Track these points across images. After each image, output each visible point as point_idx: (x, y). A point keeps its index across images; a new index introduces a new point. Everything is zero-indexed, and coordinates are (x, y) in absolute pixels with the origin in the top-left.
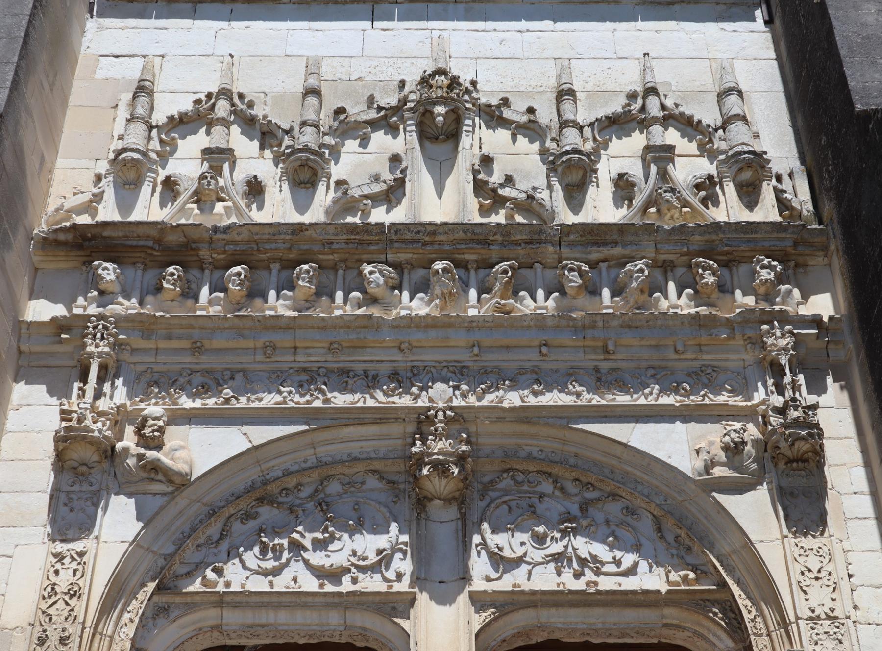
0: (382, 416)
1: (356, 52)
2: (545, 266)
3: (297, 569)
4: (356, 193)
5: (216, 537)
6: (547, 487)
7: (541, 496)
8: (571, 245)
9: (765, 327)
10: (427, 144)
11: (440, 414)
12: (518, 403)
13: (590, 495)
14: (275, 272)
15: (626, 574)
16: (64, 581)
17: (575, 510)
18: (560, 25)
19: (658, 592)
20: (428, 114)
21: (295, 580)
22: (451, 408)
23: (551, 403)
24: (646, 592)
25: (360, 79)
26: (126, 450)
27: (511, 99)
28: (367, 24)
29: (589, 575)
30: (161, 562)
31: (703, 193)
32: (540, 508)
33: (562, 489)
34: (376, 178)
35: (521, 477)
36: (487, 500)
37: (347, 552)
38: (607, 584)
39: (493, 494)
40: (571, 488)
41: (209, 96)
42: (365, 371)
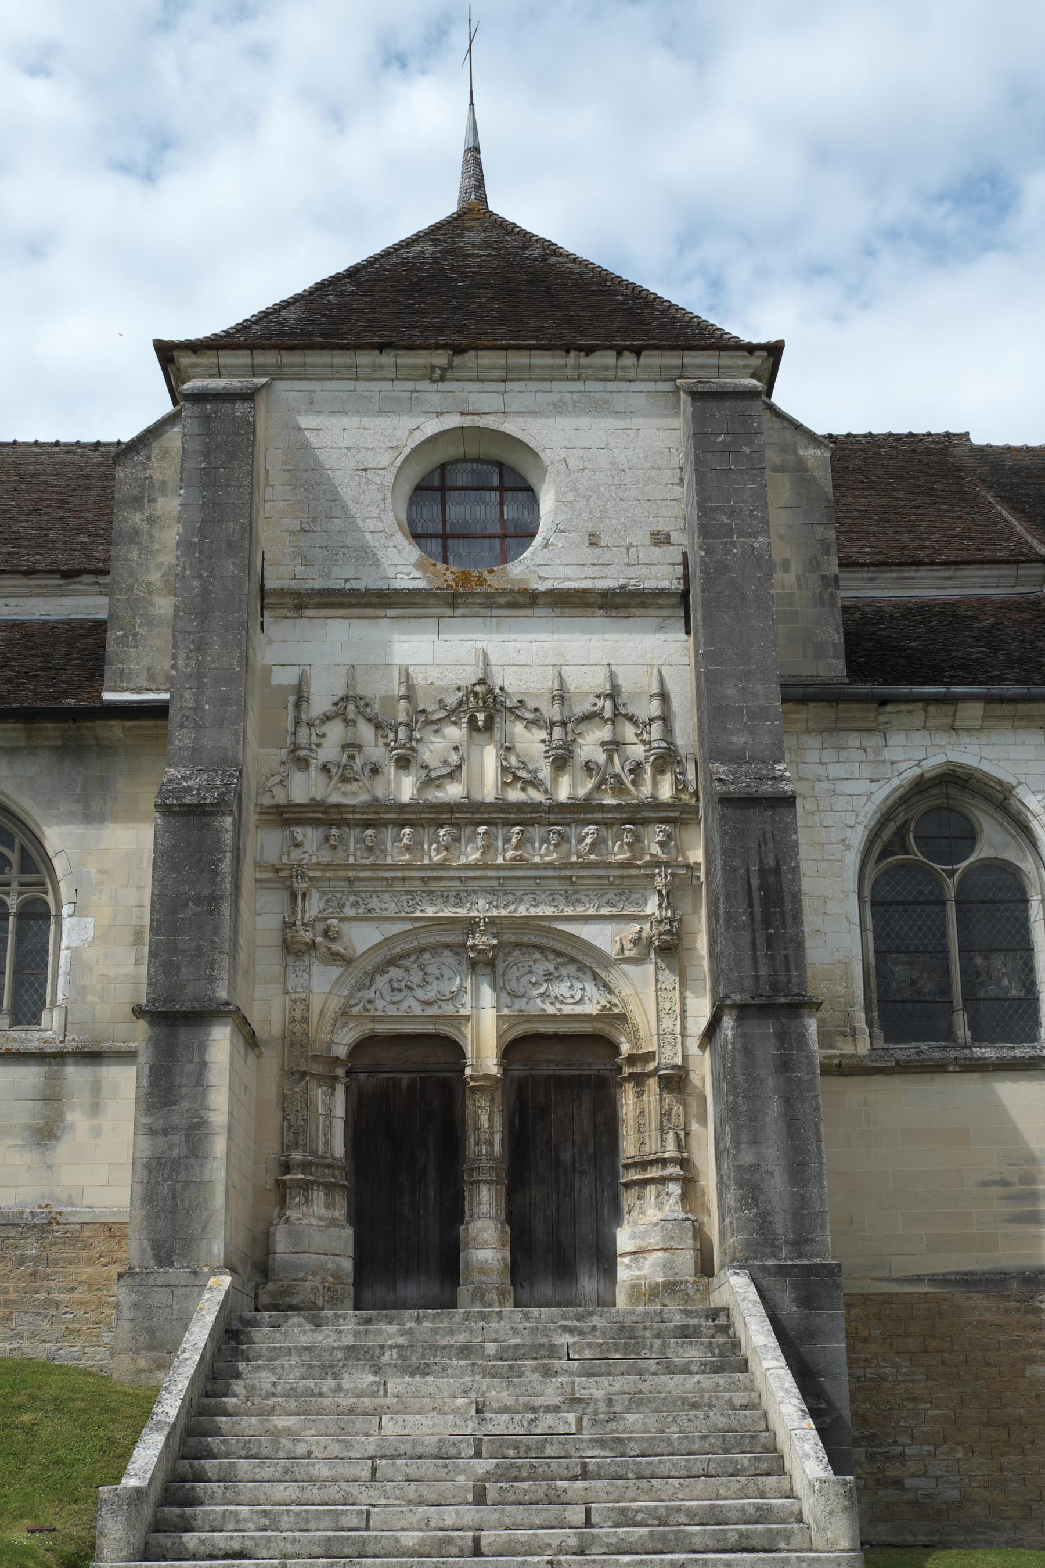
0: (452, 921)
1: (429, 661)
2: (540, 824)
3: (410, 1002)
4: (433, 775)
5: (368, 984)
6: (538, 956)
7: (535, 961)
8: (554, 813)
9: (657, 871)
10: (474, 734)
11: (482, 923)
12: (525, 914)
13: (560, 960)
14: (390, 830)
15: (576, 1003)
16: (298, 1014)
17: (552, 969)
18: (556, 637)
19: (591, 1015)
20: (472, 720)
21: (410, 1007)
22: (488, 917)
23: (541, 914)
24: (585, 1015)
25: (432, 683)
26: (321, 943)
27: (525, 699)
28: (435, 637)
29: (558, 1005)
30: (343, 1000)
31: (633, 776)
32: (534, 968)
33: (546, 957)
34: (445, 763)
35: (524, 949)
36: (507, 963)
37: (435, 992)
38: (567, 1010)
39: (510, 959)
40: (551, 957)
41: (342, 699)
42: (442, 891)
